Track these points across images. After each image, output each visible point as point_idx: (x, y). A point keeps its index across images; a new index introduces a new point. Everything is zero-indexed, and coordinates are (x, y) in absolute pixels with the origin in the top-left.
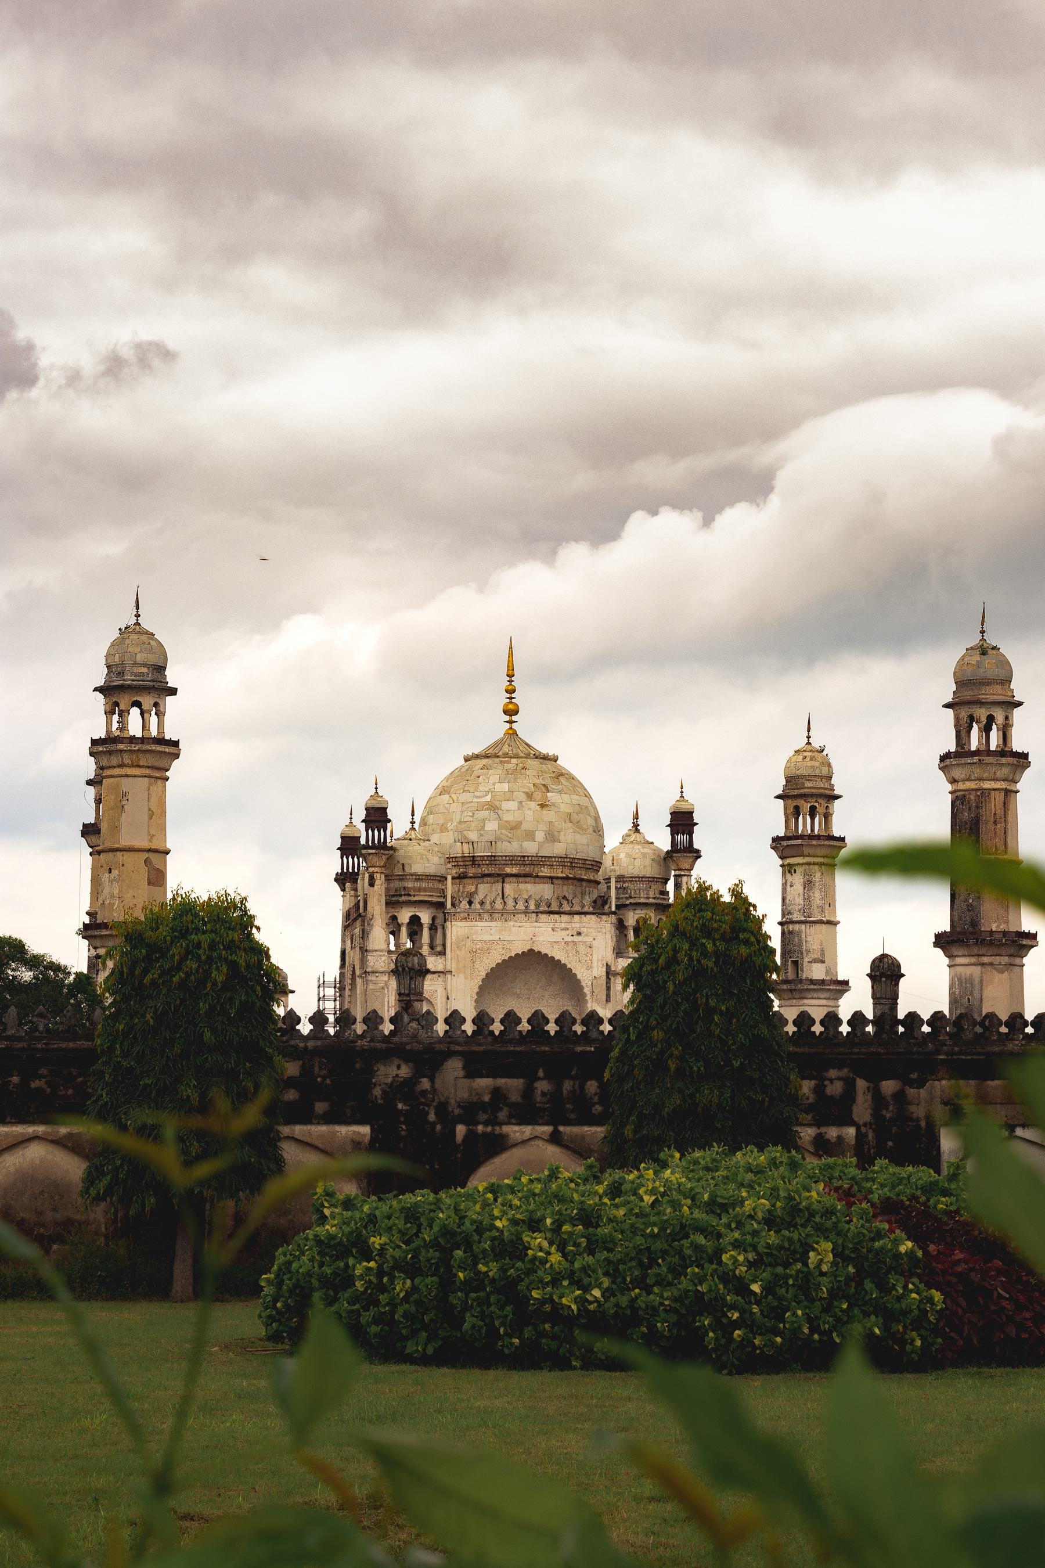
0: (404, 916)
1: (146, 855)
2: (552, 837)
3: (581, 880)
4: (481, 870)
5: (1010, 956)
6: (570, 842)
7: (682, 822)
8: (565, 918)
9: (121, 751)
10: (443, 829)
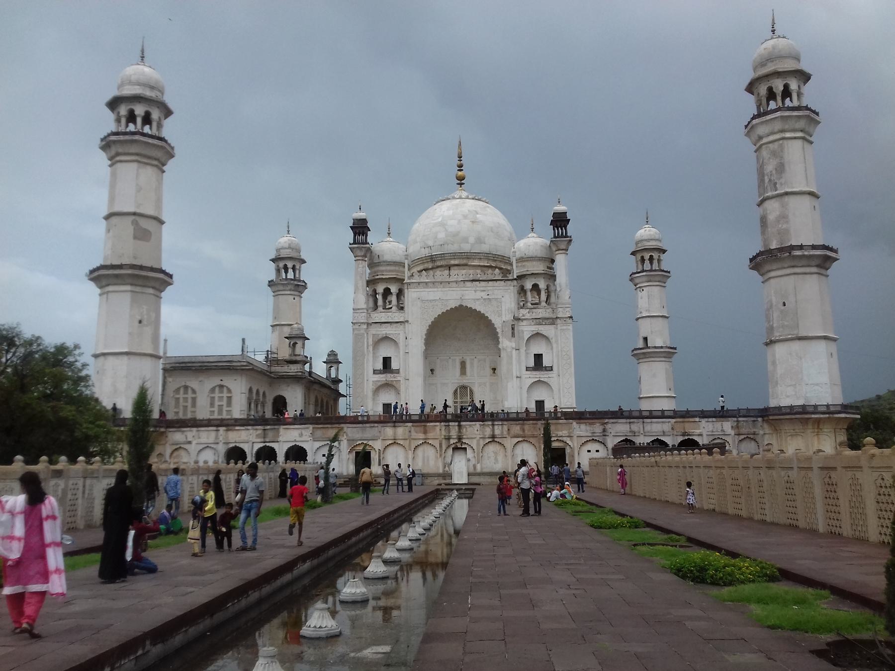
0: (380, 289)
1: (133, 217)
2: (479, 240)
3: (500, 269)
4: (436, 263)
5: (817, 266)
8: (483, 284)
9: (114, 142)
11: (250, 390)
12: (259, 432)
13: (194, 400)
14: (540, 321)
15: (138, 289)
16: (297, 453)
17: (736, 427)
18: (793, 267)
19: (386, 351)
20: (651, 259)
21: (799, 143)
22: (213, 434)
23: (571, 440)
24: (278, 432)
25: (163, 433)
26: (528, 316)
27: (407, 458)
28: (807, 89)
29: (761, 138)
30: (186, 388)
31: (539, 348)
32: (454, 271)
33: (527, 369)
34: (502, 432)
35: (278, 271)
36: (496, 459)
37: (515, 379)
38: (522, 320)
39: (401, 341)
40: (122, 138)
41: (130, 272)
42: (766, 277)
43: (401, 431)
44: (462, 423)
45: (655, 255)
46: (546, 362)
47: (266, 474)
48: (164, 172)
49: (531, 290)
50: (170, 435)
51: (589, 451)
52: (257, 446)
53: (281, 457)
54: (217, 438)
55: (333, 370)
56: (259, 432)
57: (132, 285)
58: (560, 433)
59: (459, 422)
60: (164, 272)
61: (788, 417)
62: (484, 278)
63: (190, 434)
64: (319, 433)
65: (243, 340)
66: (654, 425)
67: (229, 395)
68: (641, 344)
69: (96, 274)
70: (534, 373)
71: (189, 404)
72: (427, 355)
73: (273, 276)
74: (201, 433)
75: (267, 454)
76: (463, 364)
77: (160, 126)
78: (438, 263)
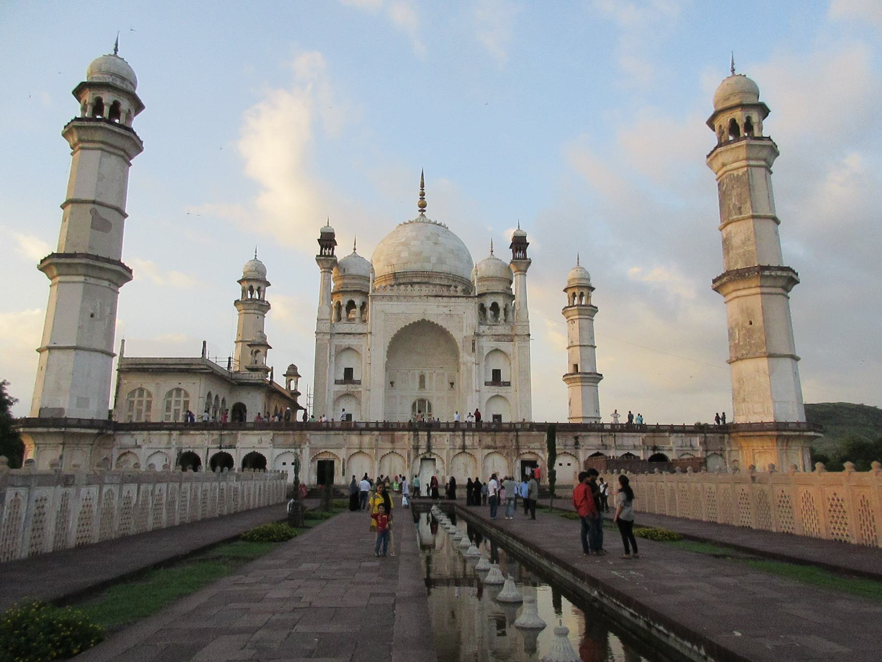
0: (344, 301)
1: (92, 206)
2: (441, 261)
6: (450, 266)
7: (519, 244)
8: (445, 299)
9: (77, 127)
10: (378, 260)
11: (209, 395)
12: (216, 437)
13: (149, 403)
14: (499, 338)
15: (92, 281)
16: (256, 461)
17: (704, 443)
18: (761, 286)
19: (347, 361)
20: (582, 295)
21: (763, 170)
22: (165, 439)
23: (543, 453)
24: (236, 437)
25: (110, 435)
26: (488, 332)
27: (372, 468)
28: (766, 122)
29: (724, 165)
30: (141, 390)
31: (497, 363)
32: (416, 287)
33: (486, 384)
34: (473, 444)
35: (244, 292)
36: (466, 471)
37: (474, 393)
38: (482, 336)
39: (364, 351)
40: (86, 124)
41: (84, 261)
42: (729, 297)
43: (367, 439)
44: (432, 433)
45: (585, 292)
46: (504, 378)
47: (217, 484)
48: (130, 165)
49: (491, 309)
50: (118, 438)
51: (561, 465)
52: (212, 453)
53: (237, 464)
54: (169, 442)
55: (293, 383)
56: (216, 437)
57: (85, 275)
58: (532, 446)
59: (429, 432)
60: (123, 265)
61: (758, 433)
62: (447, 294)
63: (140, 437)
64: (280, 440)
65: (204, 343)
66: (626, 439)
67: (187, 399)
68: (571, 371)
69: (47, 262)
70: (493, 387)
71: (144, 408)
72: (387, 368)
73: (240, 298)
74: (152, 437)
75: (222, 461)
76: (422, 378)
77: (129, 118)
78: (401, 281)
